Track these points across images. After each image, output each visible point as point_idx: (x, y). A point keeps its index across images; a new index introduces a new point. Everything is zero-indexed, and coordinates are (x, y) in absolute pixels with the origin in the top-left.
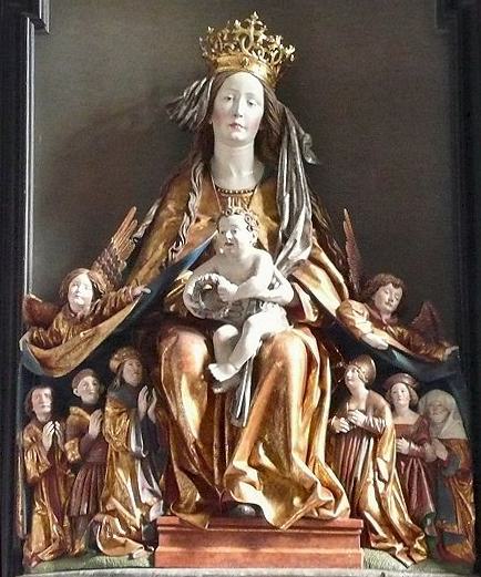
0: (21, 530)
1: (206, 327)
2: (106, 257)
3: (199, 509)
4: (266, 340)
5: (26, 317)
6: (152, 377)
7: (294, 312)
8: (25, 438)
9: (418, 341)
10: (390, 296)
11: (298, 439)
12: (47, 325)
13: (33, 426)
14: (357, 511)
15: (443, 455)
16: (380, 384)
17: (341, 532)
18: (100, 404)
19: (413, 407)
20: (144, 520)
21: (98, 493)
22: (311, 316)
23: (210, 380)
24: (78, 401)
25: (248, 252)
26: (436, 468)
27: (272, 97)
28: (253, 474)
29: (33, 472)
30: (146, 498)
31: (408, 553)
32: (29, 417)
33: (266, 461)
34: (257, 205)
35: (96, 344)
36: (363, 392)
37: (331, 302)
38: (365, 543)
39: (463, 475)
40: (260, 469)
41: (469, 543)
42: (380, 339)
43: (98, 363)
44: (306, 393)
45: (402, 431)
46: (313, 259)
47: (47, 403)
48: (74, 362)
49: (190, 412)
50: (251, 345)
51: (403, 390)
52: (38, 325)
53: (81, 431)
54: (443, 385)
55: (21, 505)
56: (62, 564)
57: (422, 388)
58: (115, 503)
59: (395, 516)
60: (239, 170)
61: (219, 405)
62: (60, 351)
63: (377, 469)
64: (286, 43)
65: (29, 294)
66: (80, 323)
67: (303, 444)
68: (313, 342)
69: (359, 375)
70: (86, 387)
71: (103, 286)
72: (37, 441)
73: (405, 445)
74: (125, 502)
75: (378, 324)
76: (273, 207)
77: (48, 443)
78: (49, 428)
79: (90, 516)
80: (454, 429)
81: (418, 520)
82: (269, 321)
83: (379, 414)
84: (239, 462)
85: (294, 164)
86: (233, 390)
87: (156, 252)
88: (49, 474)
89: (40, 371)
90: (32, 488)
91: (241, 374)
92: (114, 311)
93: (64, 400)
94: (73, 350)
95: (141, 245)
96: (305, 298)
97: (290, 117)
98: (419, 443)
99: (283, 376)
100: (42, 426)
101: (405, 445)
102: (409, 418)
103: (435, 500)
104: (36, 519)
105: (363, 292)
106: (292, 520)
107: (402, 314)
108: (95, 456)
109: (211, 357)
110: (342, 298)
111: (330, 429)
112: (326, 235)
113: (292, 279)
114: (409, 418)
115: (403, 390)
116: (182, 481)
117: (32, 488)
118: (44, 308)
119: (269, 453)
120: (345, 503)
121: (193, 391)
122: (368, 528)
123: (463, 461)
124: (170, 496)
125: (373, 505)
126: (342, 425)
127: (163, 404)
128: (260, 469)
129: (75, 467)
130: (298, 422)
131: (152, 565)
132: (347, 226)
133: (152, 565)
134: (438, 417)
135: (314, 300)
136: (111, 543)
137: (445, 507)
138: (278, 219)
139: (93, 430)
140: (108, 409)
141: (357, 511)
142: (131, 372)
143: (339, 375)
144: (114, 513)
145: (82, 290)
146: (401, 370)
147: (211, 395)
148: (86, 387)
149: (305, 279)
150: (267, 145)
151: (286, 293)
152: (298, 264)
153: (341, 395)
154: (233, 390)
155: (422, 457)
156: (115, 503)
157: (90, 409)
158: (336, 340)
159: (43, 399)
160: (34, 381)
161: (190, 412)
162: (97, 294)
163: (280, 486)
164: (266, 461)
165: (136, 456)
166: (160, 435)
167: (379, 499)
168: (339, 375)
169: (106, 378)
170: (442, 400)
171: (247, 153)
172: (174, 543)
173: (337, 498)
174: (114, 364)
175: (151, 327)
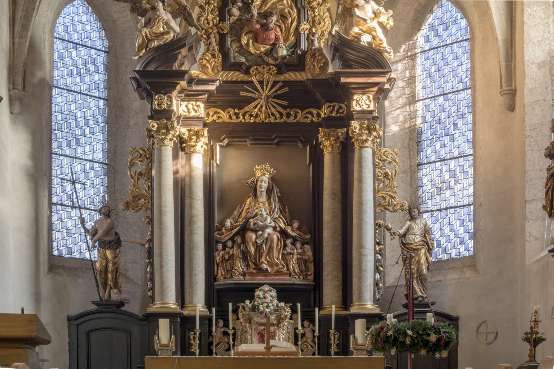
0: (216, 273)
1: (255, 231)
2: (233, 216)
3: (254, 269)
4: (269, 234)
5: (215, 229)
6: (243, 242)
7: (275, 228)
8: (216, 254)
9: (302, 234)
10: (296, 225)
11: (275, 255)
12: (220, 230)
13: (218, 252)
14: (288, 269)
15: (307, 258)
16: (293, 244)
17: (285, 274)
18: (233, 247)
19: (301, 248)
20: (243, 271)
21: (232, 266)
22: (279, 229)
23: (257, 243)
24: (228, 247)
25: (265, 216)
26: (306, 261)
27: (270, 181)
28: (266, 262)
29: (218, 261)
30: (243, 267)
31: (299, 278)
32: (217, 250)
33: (268, 259)
34: (267, 205)
35: (232, 235)
36: (290, 245)
37: (283, 226)
38: (290, 276)
39: (311, 262)
40: (268, 261)
41: (312, 276)
42: (294, 234)
43: (232, 239)
44: (277, 245)
45: (298, 254)
46: (279, 217)
47: (221, 247)
48: (227, 238)
49: (252, 249)
50: (266, 235)
51: (298, 245)
52: (218, 230)
53: (229, 253)
54: (307, 243)
55: (215, 268)
56: (225, 280)
57: (303, 244)
58: (236, 268)
59: (296, 270)
60: (263, 198)
61: (258, 247)
62: (224, 236)
63: (292, 261)
64: (274, 170)
65: (216, 224)
66: (228, 230)
67: (277, 256)
68: (279, 235)
69: (289, 242)
70: (230, 244)
71: (233, 223)
72: (219, 255)
73: (299, 256)
74: (238, 267)
75: (293, 231)
76: (270, 204)
77: (221, 255)
78: (222, 252)
79: (231, 270)
80: (310, 253)
81: (301, 271)
82: (269, 230)
83: (293, 250)
84: (263, 260)
85: (275, 196)
86: (262, 244)
87: (244, 214)
88: (222, 262)
89: (219, 240)
90: (218, 265)
91: (263, 241)
92: (235, 228)
93: (225, 246)
94: (226, 236)
95: (241, 213)
96: (277, 225)
97: (274, 185)
98: (302, 256)
99: (272, 241)
100: (220, 252)
101: (299, 256)
102: (300, 251)
103: (305, 267)
104: (219, 271)
105: (291, 225)
106: (274, 271)
107: (299, 228)
108: (232, 258)
109: (257, 238)
110: (285, 225)
111: (283, 253)
112: (282, 211)
113: (274, 221)
114: (300, 251)
115: (298, 245)
116: (250, 263)
117: (218, 265)
118: (220, 226)
119: (269, 258)
120: (285, 268)
121: (253, 245)
122: (290, 273)
123: (312, 259)
124: (248, 266)
125: (292, 268)
126: (285, 252)
127: (246, 248)
128: (268, 261)
129: (227, 260)
130: (275, 251)
131: (245, 280)
132: (287, 210)
133: (245, 280)
134: (306, 250)
135: (279, 226)
136: (236, 276)
137: (307, 269)
138: (271, 208)
139: (231, 253)
140: (235, 248)
141: (288, 269)
142: (239, 241)
143: (284, 241)
144: (236, 270)
145: (228, 223)
146: (298, 241)
147: (257, 246)
148: (230, 244)
149: (277, 221)
150: (269, 191)
151: (273, 224)
152: (276, 218)
153: (285, 246)
154: (262, 244)
155: (302, 259)
156: (236, 268)
157: (230, 248)
158: (284, 234)
159: (220, 246)
160: (217, 242)
161: (252, 249)
162: (231, 224)
163: (271, 264)
164: (268, 259)
165: (240, 258)
166: (245, 255)
167: (293, 267)
168: (284, 241)
169: (234, 242)
170: (306, 246)
171: (264, 194)
172: (249, 276)
173: (284, 267)
174: (235, 239)
175: (244, 229)
